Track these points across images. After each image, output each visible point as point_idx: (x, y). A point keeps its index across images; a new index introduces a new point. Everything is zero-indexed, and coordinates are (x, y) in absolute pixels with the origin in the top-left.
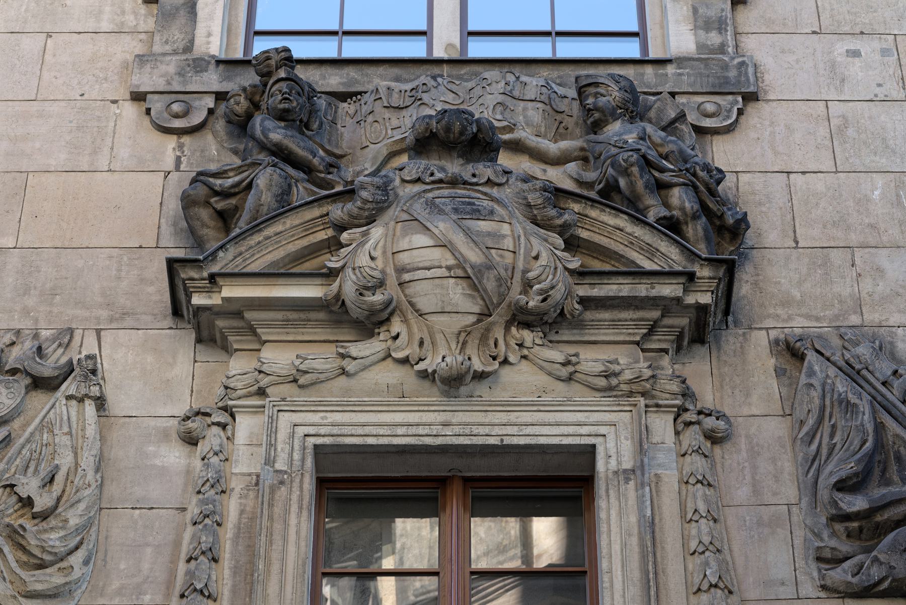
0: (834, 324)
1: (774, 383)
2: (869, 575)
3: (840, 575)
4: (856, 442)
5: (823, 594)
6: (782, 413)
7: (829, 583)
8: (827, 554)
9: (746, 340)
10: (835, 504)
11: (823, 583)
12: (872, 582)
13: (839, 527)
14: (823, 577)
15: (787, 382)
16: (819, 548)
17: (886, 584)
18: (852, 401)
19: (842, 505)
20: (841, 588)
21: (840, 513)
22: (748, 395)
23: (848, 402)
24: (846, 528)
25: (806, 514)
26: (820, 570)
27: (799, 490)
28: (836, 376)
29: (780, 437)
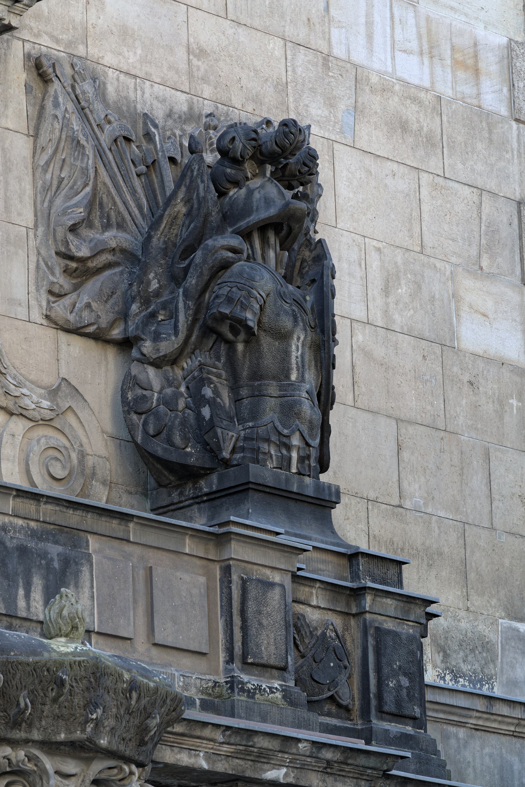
0: (67, 51)
1: (23, 97)
2: (81, 317)
3: (61, 310)
4: (79, 183)
5: (44, 322)
6: (26, 132)
7: (53, 315)
8: (56, 290)
9: (9, 47)
10: (66, 243)
11: (48, 313)
12: (83, 325)
13: (63, 262)
14: (50, 308)
15: (32, 101)
16: (53, 283)
17: (91, 329)
18: (81, 142)
19: (72, 247)
20: (60, 323)
21: (68, 253)
22: (6, 106)
23: (78, 142)
24: (67, 265)
25: (41, 243)
26: (48, 302)
27: (36, 215)
28: (73, 113)
29: (24, 157)
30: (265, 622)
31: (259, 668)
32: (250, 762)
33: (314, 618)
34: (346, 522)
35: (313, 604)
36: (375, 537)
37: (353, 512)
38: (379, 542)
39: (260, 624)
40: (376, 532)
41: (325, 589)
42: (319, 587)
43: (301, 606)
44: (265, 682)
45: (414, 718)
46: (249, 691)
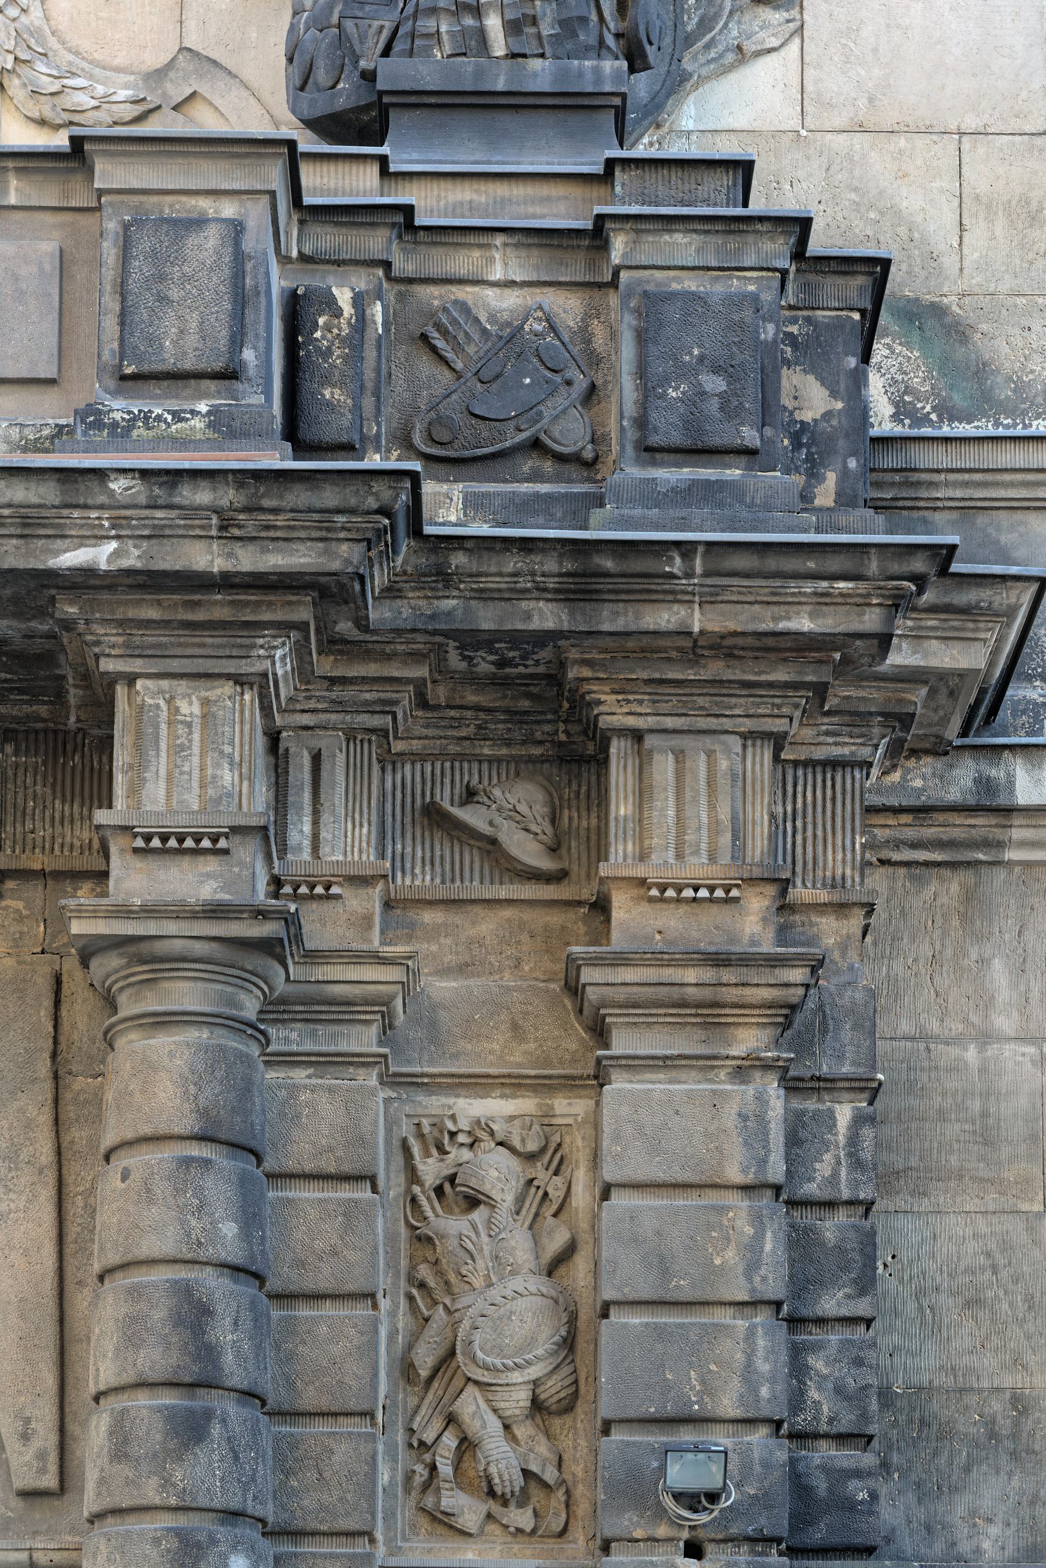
30: (175, 294)
31: (165, 383)
32: (14, 541)
33: (505, 305)
34: (899, 182)
35: (492, 278)
36: (977, 198)
37: (919, 162)
38: (989, 207)
39: (163, 299)
40: (983, 188)
41: (517, 246)
42: (505, 245)
43: (469, 289)
44: (158, 405)
45: (751, 452)
46: (115, 425)
